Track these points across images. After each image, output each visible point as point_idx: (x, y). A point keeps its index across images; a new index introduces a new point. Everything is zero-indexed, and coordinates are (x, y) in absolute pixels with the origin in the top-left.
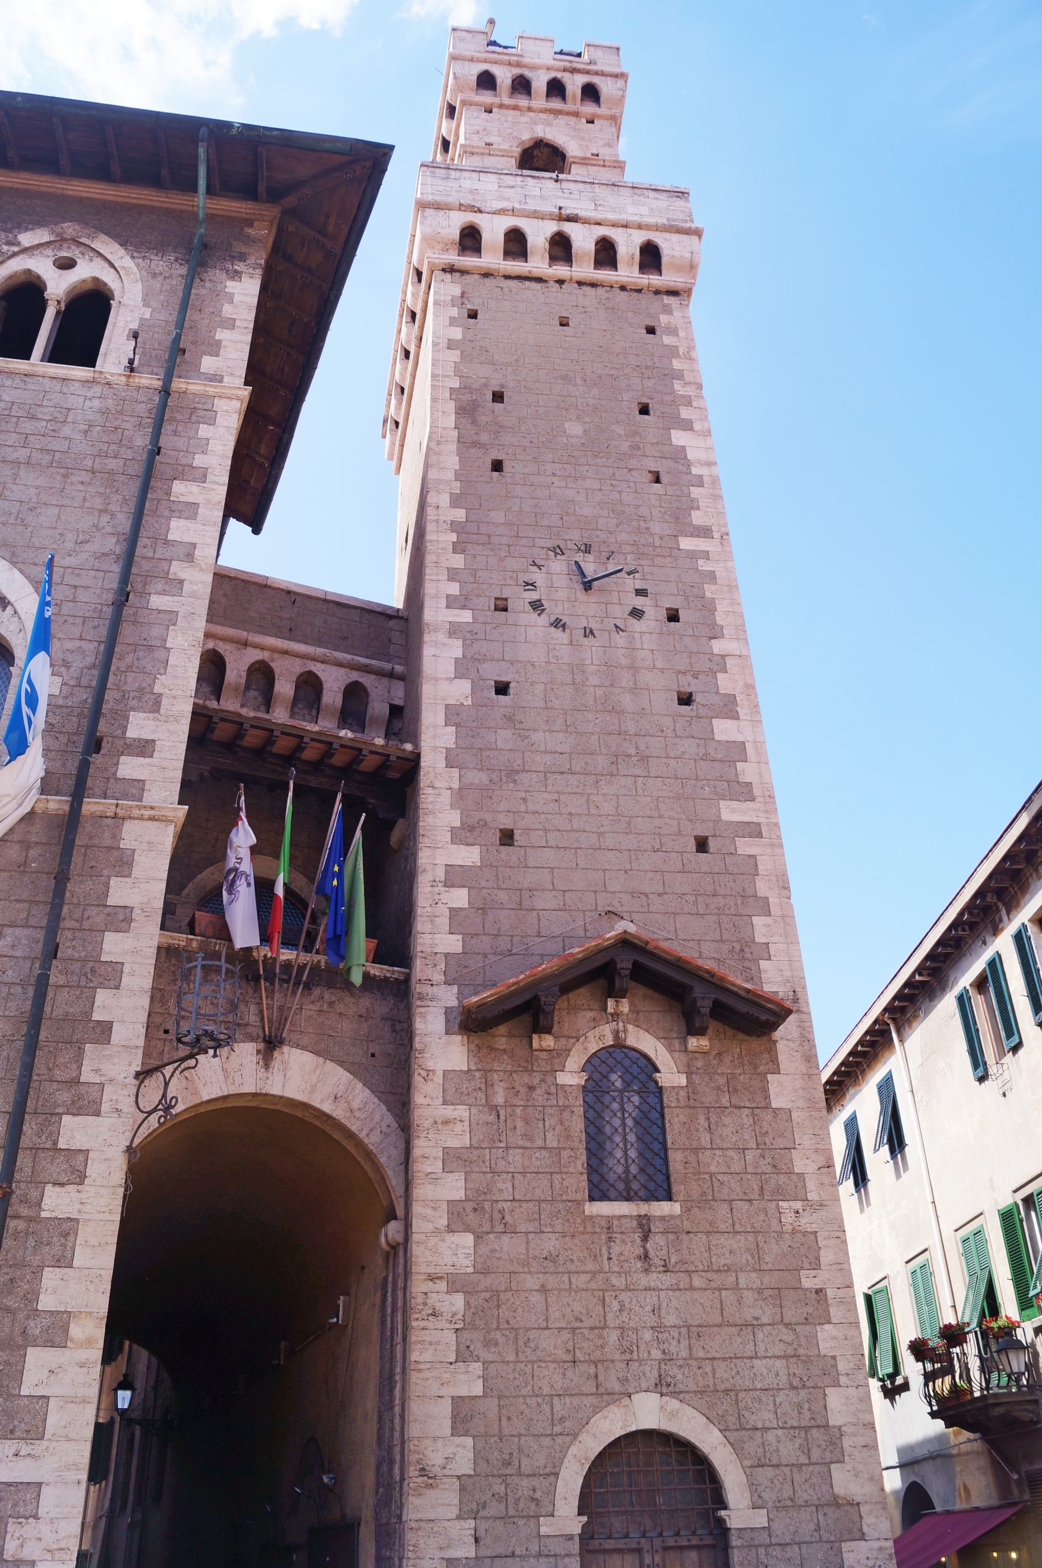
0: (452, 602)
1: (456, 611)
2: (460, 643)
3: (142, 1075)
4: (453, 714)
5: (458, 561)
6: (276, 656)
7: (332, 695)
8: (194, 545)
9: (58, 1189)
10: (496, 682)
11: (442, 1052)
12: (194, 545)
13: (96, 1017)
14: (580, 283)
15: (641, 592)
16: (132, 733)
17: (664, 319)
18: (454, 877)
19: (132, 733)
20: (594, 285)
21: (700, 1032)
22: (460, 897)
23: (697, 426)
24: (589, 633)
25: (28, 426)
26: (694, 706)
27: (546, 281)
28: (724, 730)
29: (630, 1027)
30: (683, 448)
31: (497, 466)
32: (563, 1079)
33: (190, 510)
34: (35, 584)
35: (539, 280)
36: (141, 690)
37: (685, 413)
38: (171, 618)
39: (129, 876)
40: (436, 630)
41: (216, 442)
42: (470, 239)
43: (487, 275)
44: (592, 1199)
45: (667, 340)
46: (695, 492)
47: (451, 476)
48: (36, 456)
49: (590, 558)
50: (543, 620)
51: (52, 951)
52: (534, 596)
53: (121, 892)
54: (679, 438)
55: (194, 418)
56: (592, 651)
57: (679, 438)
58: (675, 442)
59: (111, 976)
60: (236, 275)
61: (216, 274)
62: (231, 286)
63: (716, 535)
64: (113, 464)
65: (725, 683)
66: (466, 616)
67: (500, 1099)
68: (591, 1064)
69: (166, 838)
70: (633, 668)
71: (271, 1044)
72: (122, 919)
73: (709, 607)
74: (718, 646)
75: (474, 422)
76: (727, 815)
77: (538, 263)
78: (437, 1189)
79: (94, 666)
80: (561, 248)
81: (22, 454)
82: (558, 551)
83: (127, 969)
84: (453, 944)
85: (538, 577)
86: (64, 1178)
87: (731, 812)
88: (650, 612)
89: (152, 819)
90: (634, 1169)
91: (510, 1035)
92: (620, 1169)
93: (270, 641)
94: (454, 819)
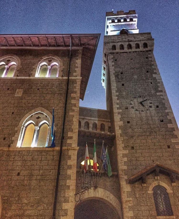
0: (118, 108)
1: (118, 110)
2: (120, 115)
3: (76, 195)
4: (120, 127)
5: (118, 101)
6: (89, 120)
8: (76, 104)
9: (63, 217)
10: (127, 121)
11: (126, 188)
12: (76, 104)
13: (67, 185)
14: (133, 52)
16: (69, 135)
17: (149, 56)
18: (124, 156)
19: (69, 135)
20: (136, 52)
21: (175, 182)
22: (125, 159)
23: (157, 73)
25: (47, 88)
26: (164, 122)
27: (127, 52)
29: (160, 182)
30: (155, 77)
31: (123, 85)
32: (149, 192)
34: (51, 113)
35: (126, 52)
36: (70, 129)
37: (155, 71)
38: (73, 116)
39: (71, 159)
40: (116, 113)
41: (78, 87)
42: (114, 47)
43: (117, 53)
44: (158, 215)
46: (158, 84)
47: (115, 87)
48: (49, 92)
49: (141, 98)
51: (59, 173)
52: (132, 106)
55: (73, 83)
56: (143, 114)
57: (154, 76)
58: (154, 76)
59: (69, 177)
60: (77, 59)
61: (74, 59)
62: (77, 61)
63: (163, 91)
64: (61, 92)
66: (121, 111)
67: (138, 196)
68: (153, 189)
69: (76, 152)
70: (151, 116)
71: (96, 187)
72: (70, 167)
73: (164, 104)
75: (118, 78)
76: (173, 141)
77: (126, 50)
79: (62, 125)
80: (130, 47)
81: (47, 92)
82: (135, 98)
83: (71, 176)
84: (125, 167)
85: (132, 102)
86: (64, 214)
88: (153, 106)
89: (73, 150)
90: (165, 210)
91: (138, 184)
92: (162, 209)
93: (88, 118)
94: (123, 145)
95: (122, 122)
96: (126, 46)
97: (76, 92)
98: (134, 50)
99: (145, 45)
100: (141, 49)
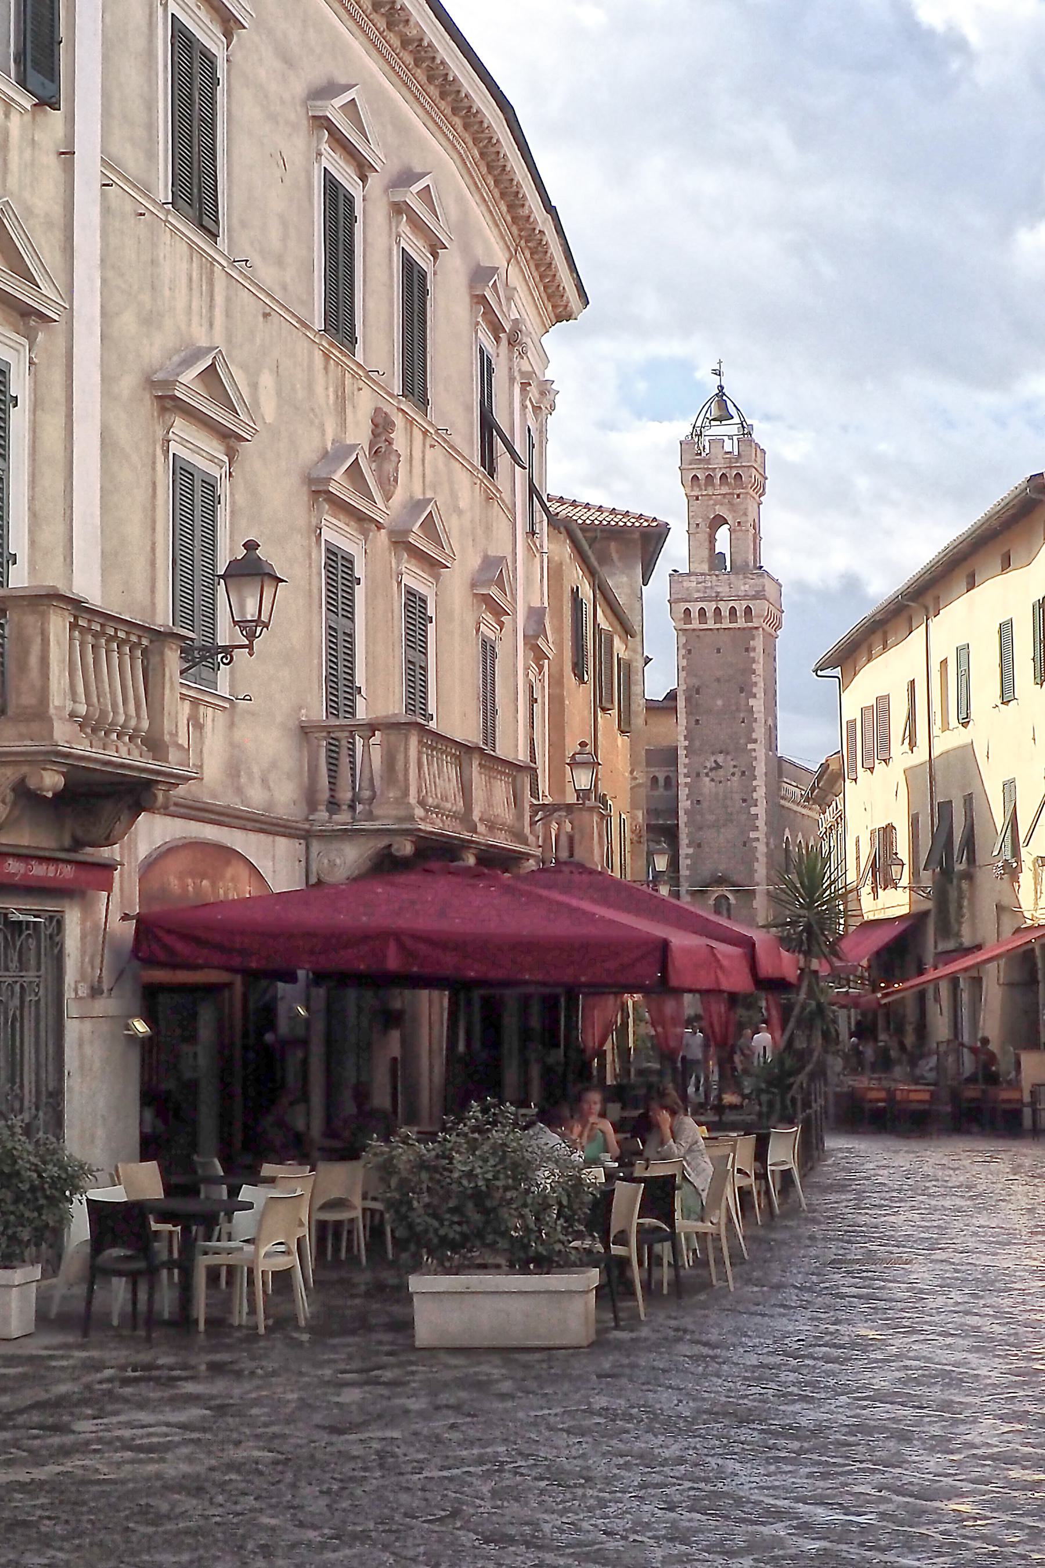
5: (687, 761)
7: (661, 782)
15: (735, 766)
18: (687, 856)
22: (689, 862)
24: (720, 782)
43: (694, 630)
45: (752, 654)
50: (708, 779)
54: (752, 702)
66: (689, 780)
74: (755, 783)
84: (687, 873)
87: (752, 835)
94: (686, 841)
95: (689, 802)
98: (726, 624)
100: (741, 623)
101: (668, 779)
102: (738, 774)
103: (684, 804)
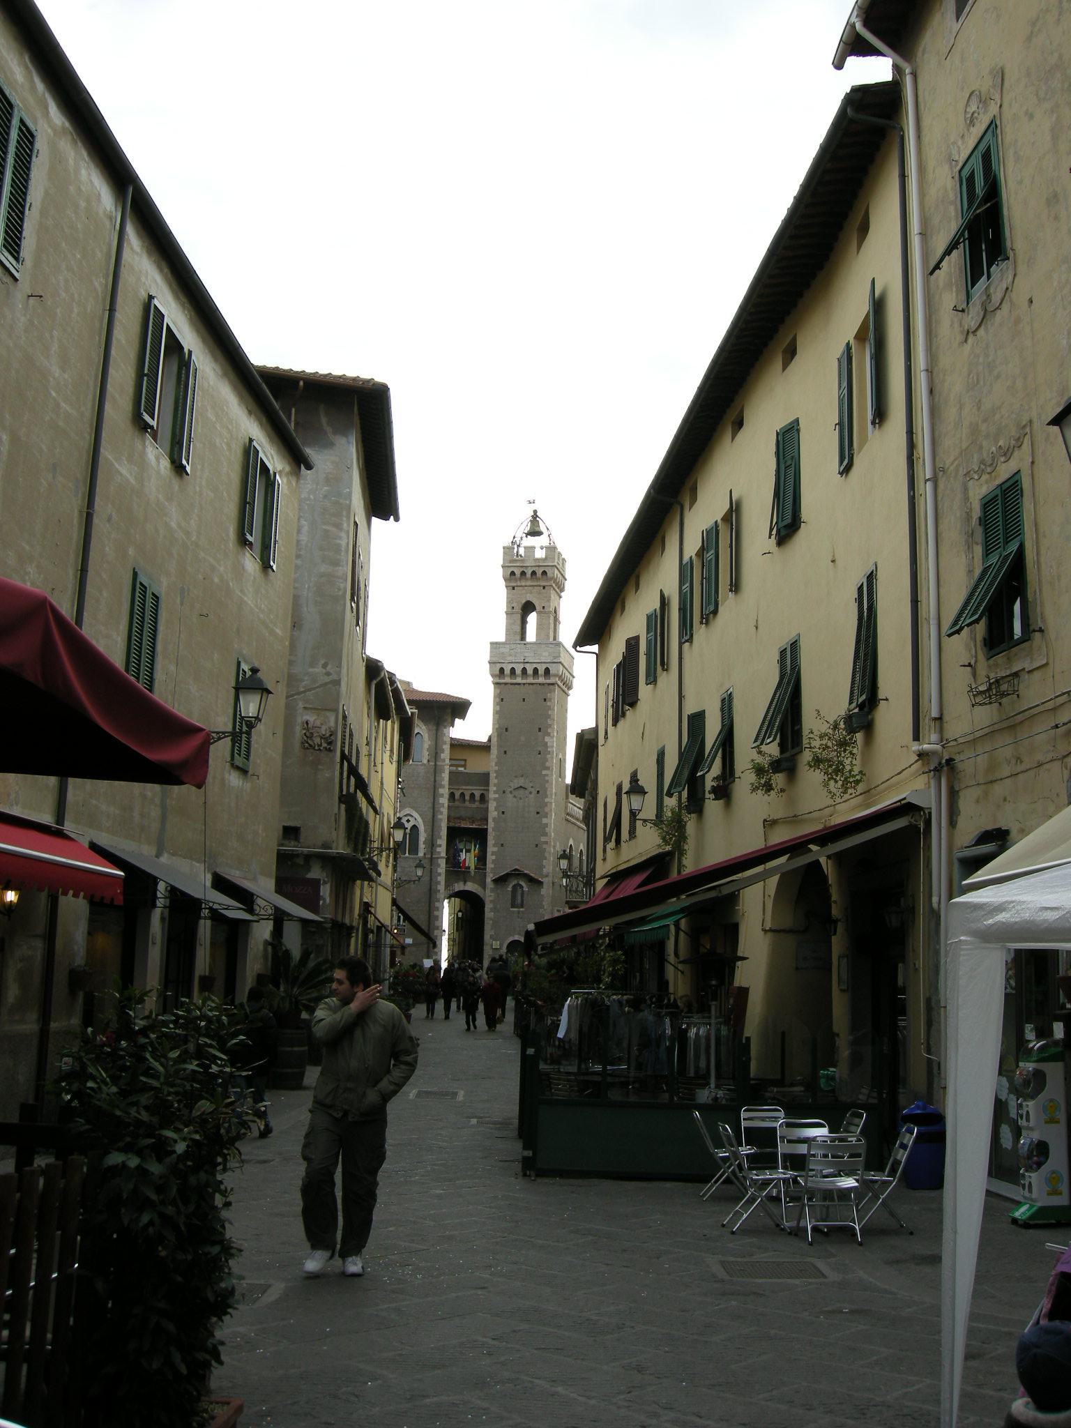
4: (494, 819)
7: (477, 798)
18: (493, 853)
28: (545, 821)
33: (442, 795)
42: (502, 670)
53: (440, 870)
54: (547, 739)
59: (439, 883)
65: (546, 810)
78: (488, 907)
87: (543, 839)
96: (518, 672)
97: (443, 787)
98: (531, 680)
99: (547, 671)
101: (482, 796)
102: (534, 792)
103: (493, 814)
